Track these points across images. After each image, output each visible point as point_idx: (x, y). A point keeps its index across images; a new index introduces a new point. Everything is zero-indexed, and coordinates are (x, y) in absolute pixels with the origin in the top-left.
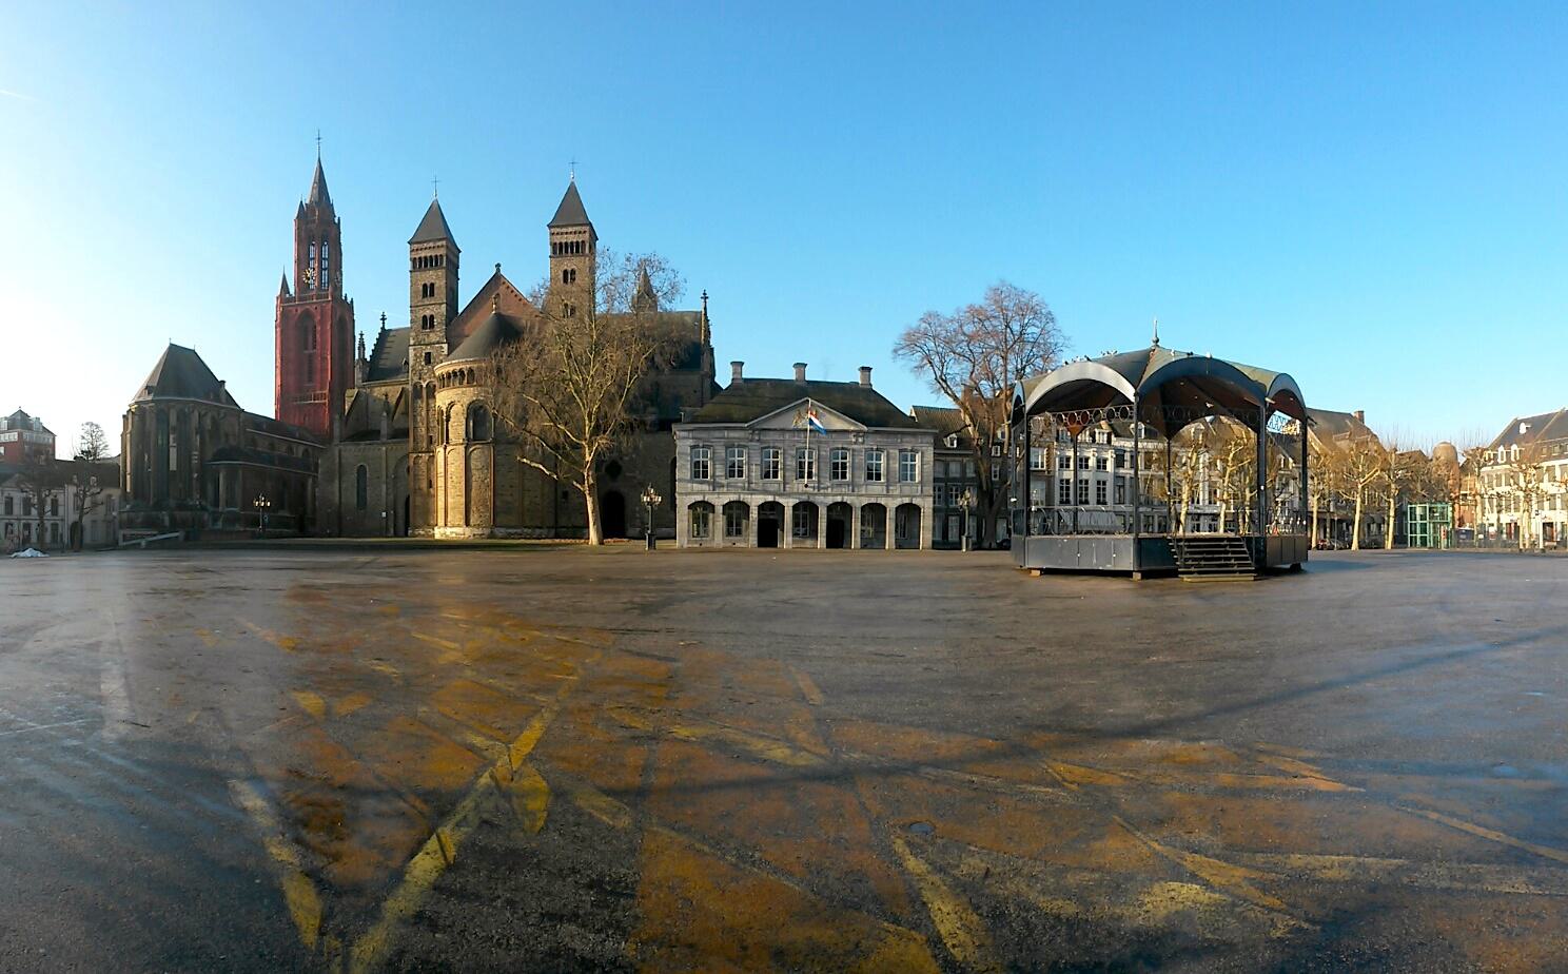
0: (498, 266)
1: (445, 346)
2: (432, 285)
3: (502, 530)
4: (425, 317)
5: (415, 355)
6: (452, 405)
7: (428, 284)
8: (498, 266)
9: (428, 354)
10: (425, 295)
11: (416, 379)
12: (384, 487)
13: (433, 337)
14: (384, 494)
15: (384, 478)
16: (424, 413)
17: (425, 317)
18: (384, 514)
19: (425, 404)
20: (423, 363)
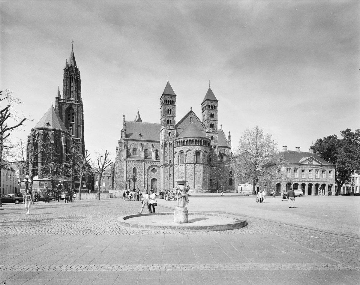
0: (191, 108)
1: (176, 131)
2: (171, 110)
3: (205, 190)
4: (168, 120)
5: (165, 132)
6: (188, 151)
7: (170, 110)
8: (191, 108)
9: (170, 133)
10: (168, 113)
11: (166, 140)
13: (171, 127)
14: (143, 178)
16: (168, 152)
17: (168, 120)
18: (144, 185)
20: (168, 135)
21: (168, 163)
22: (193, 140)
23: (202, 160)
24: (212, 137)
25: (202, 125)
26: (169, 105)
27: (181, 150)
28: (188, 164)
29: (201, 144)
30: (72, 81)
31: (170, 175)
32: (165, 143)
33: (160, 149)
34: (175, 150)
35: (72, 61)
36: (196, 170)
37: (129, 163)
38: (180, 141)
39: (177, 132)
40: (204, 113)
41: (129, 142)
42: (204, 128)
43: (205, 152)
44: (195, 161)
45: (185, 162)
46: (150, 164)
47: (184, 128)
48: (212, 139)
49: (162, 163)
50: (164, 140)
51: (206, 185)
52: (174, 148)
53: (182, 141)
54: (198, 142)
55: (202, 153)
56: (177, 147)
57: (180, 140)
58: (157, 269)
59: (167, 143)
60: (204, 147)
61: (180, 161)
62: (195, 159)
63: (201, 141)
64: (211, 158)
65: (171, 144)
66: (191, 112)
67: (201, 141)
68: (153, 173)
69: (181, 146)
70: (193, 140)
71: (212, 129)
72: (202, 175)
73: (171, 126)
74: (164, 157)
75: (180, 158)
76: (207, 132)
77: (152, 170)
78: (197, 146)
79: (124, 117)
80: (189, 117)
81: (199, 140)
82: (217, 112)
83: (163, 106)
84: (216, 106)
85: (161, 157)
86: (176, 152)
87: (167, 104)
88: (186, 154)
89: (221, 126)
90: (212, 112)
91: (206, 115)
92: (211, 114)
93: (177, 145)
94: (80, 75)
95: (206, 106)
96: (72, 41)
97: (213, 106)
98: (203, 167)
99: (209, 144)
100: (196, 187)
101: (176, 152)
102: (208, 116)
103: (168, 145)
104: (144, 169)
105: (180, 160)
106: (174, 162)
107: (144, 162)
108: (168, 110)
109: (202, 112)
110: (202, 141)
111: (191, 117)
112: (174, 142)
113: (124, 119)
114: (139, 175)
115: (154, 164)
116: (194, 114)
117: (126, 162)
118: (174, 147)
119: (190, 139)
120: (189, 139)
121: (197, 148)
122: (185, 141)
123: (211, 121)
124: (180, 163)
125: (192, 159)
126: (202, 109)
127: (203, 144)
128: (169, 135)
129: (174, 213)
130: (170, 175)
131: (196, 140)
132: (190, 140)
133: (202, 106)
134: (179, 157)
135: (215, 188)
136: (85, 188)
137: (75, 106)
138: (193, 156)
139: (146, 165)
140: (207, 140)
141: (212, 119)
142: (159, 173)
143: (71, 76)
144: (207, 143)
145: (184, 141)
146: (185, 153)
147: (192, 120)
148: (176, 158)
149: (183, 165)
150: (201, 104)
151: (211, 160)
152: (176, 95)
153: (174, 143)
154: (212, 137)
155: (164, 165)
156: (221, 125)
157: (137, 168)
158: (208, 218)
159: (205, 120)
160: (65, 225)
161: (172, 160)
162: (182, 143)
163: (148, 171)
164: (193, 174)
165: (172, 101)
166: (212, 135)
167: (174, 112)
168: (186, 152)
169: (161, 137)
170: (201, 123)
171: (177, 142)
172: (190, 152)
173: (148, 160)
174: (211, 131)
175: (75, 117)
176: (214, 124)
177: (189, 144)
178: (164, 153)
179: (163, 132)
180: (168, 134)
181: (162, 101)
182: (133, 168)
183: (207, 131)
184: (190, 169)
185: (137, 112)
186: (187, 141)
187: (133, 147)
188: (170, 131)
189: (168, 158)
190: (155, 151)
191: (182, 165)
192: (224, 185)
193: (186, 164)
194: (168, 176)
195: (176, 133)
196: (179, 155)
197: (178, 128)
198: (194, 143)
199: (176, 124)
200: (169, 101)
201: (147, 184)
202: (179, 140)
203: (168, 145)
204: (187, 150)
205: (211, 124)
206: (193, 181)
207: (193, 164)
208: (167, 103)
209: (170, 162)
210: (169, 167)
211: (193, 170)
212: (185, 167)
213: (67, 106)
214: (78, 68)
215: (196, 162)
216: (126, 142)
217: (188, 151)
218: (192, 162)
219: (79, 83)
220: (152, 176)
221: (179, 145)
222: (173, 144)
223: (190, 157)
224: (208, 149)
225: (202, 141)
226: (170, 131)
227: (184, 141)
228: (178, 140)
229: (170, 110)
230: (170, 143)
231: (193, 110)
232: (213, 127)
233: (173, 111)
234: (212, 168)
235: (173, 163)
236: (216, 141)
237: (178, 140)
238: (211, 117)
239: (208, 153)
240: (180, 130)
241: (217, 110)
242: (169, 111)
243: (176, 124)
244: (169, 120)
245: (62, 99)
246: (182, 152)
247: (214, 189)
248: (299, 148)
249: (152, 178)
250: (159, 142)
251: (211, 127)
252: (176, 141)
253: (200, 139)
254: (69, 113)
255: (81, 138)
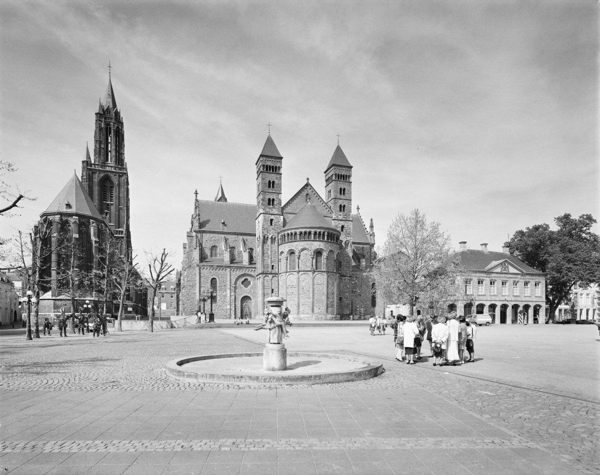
0: (308, 179)
1: (282, 217)
2: (273, 182)
3: (330, 316)
4: (269, 199)
5: (265, 219)
6: (303, 250)
7: (272, 181)
8: (308, 179)
10: (269, 187)
11: (265, 233)
12: (229, 291)
13: (275, 211)
15: (229, 286)
16: (269, 252)
17: (269, 199)
18: (229, 307)
19: (270, 248)
20: (270, 224)
21: (270, 270)
22: (310, 233)
23: (325, 265)
24: (343, 227)
25: (326, 207)
26: (270, 173)
27: (290, 249)
28: (303, 273)
29: (324, 238)
30: (110, 134)
31: (273, 290)
32: (264, 237)
33: (257, 246)
34: (281, 248)
35: (110, 100)
36: (315, 282)
37: (205, 269)
38: (288, 234)
39: (284, 219)
40: (329, 188)
41: (204, 234)
42: (329, 212)
43: (331, 251)
44: (314, 267)
45: (297, 269)
46: (239, 273)
47: (296, 213)
48: (342, 230)
49: (260, 271)
50: (263, 233)
51: (332, 306)
52: (278, 246)
53: (292, 234)
54: (319, 236)
55: (325, 254)
56: (284, 243)
57: (289, 232)
58: (206, 448)
59: (268, 237)
60: (330, 244)
61: (288, 268)
62: (314, 264)
63: (324, 233)
64: (341, 262)
65: (275, 238)
66: (307, 185)
67: (324, 233)
68: (244, 288)
69: (291, 242)
70: (310, 233)
71: (341, 213)
72: (325, 291)
73: (274, 210)
74: (263, 260)
75: (288, 261)
76: (333, 218)
77: (242, 283)
78: (316, 242)
79: (196, 193)
80: (304, 193)
81: (320, 233)
82: (350, 186)
83: (260, 175)
84: (349, 176)
85: (258, 259)
86: (282, 252)
87: (268, 173)
88: (299, 256)
89: (358, 208)
90: (342, 185)
91: (332, 191)
92: (341, 189)
93: (283, 240)
94: (122, 124)
95: (332, 176)
96: (110, 67)
97: (344, 176)
98: (328, 278)
99: (338, 238)
100: (316, 310)
101: (282, 252)
102: (335, 191)
103: (269, 240)
104: (229, 280)
105: (288, 265)
106: (278, 269)
107: (229, 269)
108: (269, 181)
109: (325, 186)
110: (326, 234)
111: (307, 194)
112: (279, 235)
113: (196, 196)
114: (221, 290)
115: (246, 272)
116: (312, 190)
117: (200, 269)
118: (280, 243)
119: (287, 232)
120: (303, 230)
121: (317, 245)
122: (298, 233)
123: (341, 201)
124: (288, 271)
125: (309, 264)
126: (326, 181)
127: (328, 239)
128: (271, 224)
129: (263, 354)
130: (273, 290)
131: (315, 233)
132: (305, 233)
133: (326, 176)
134: (287, 260)
135: (348, 312)
136: (130, 312)
137: (115, 175)
138: (311, 259)
139: (233, 273)
140: (334, 232)
141: (342, 197)
142: (255, 287)
143: (108, 124)
144: (334, 237)
145: (296, 233)
146: (297, 254)
147: (309, 199)
148: (283, 263)
149: (294, 273)
150: (325, 173)
151: (340, 266)
152: (282, 158)
153: (279, 238)
154: (343, 227)
155: (262, 273)
156: (358, 207)
157: (218, 280)
158: (321, 362)
159: (330, 199)
160: (77, 374)
161: (276, 265)
162: (292, 237)
163: (236, 283)
164: (309, 288)
165: (276, 167)
166: (342, 223)
167: (280, 185)
168: (300, 253)
169: (257, 227)
170: (324, 205)
171: (285, 235)
172: (305, 252)
173: (236, 265)
174: (340, 217)
175: (115, 193)
176: (346, 205)
177: (294, 240)
178: (263, 254)
179: (261, 218)
180: (269, 222)
181: (259, 167)
182: (210, 279)
183: (334, 217)
184: (307, 279)
185: (218, 186)
186: (301, 233)
187: (212, 243)
188: (272, 217)
189: (269, 261)
190: (248, 251)
191: (293, 273)
192: (362, 308)
193: (299, 271)
194: (270, 291)
195: (282, 220)
196: (287, 258)
197: (284, 211)
198: (312, 238)
199: (283, 205)
200: (270, 166)
201: (234, 305)
202: (287, 232)
203: (269, 240)
204: (300, 248)
205: (341, 205)
206: (311, 300)
207: (311, 271)
208: (267, 170)
209: (273, 269)
210: (270, 276)
211: (311, 282)
212: (297, 276)
213: (102, 175)
214: (119, 111)
215: (316, 269)
216: (199, 235)
217: (303, 250)
218: (310, 269)
219: (121, 137)
220: (243, 291)
221: (287, 240)
222: (277, 239)
223: (306, 260)
224: (334, 247)
225: (326, 234)
226: (272, 217)
227: (296, 233)
228: (286, 233)
229: (272, 181)
230: (272, 238)
231: (310, 182)
232: (344, 211)
233: (278, 184)
234: (343, 278)
235: (277, 270)
236: (348, 234)
237: (286, 233)
238: (341, 194)
239: (336, 253)
240: (289, 215)
241: (351, 182)
242: (271, 184)
243: (282, 205)
244: (271, 199)
245: (94, 164)
246: (292, 253)
247: (345, 313)
248: (486, 245)
249: (242, 296)
250: (255, 235)
251: (341, 210)
252: (283, 233)
253: (322, 231)
254: (105, 186)
255: (125, 228)
